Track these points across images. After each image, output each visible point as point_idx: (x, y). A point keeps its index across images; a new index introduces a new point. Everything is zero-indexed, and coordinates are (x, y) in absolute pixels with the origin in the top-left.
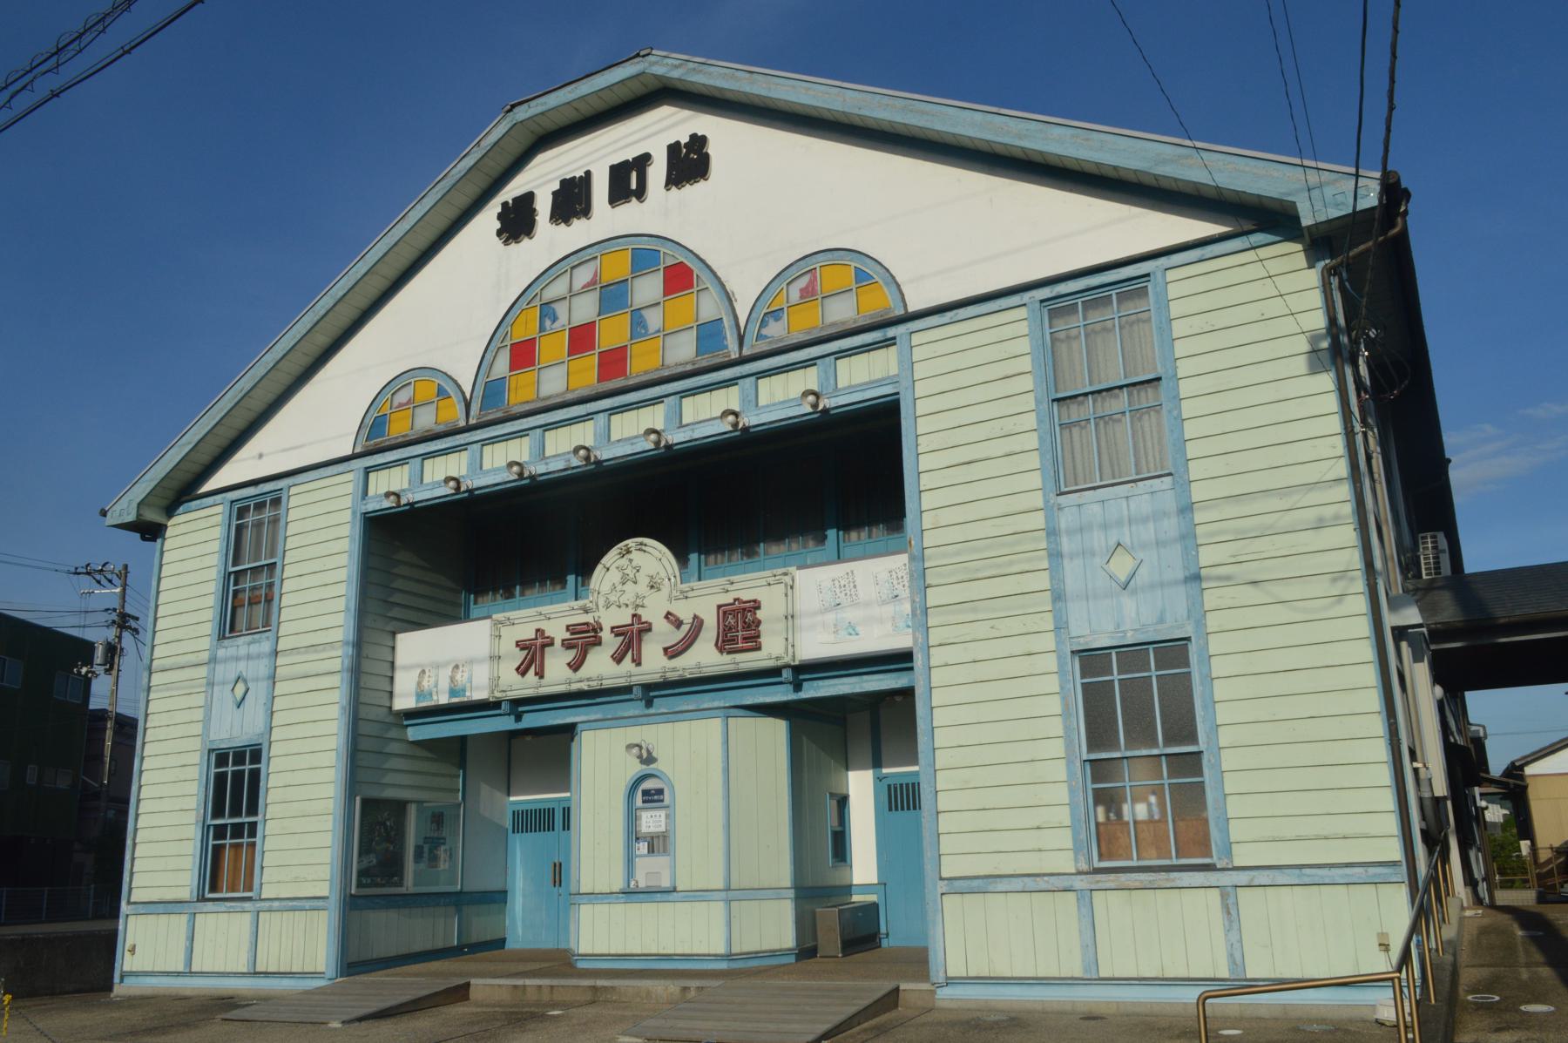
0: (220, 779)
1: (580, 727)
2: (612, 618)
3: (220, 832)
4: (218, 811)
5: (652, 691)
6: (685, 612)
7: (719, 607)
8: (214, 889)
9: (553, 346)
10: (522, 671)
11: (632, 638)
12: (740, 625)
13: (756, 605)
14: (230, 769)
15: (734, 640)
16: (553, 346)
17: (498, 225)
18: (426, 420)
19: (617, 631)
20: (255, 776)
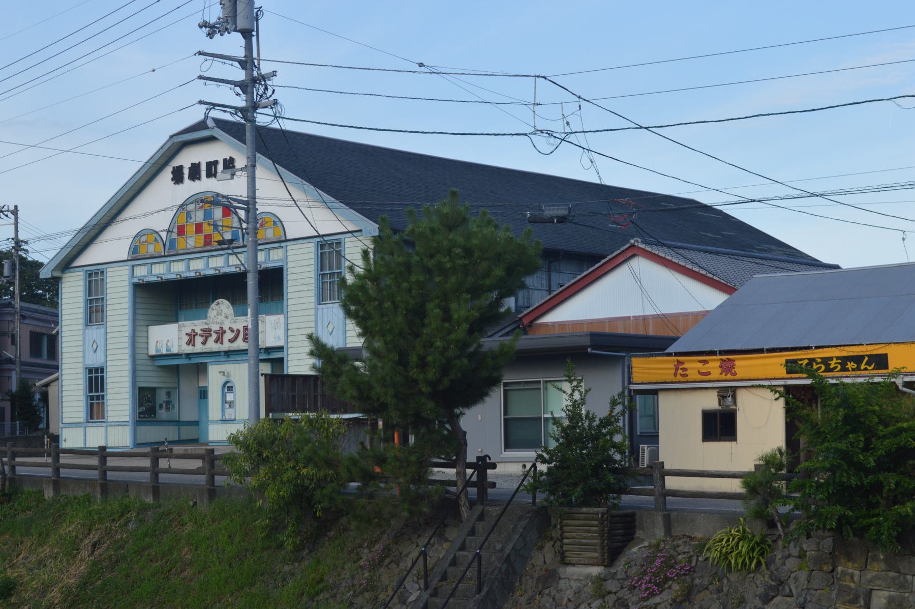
0: (90, 378)
2: (215, 327)
3: (92, 398)
4: (91, 391)
5: (228, 353)
8: (92, 418)
9: (190, 229)
10: (188, 343)
14: (94, 375)
16: (190, 229)
17: (171, 176)
18: (151, 249)
20: (102, 378)
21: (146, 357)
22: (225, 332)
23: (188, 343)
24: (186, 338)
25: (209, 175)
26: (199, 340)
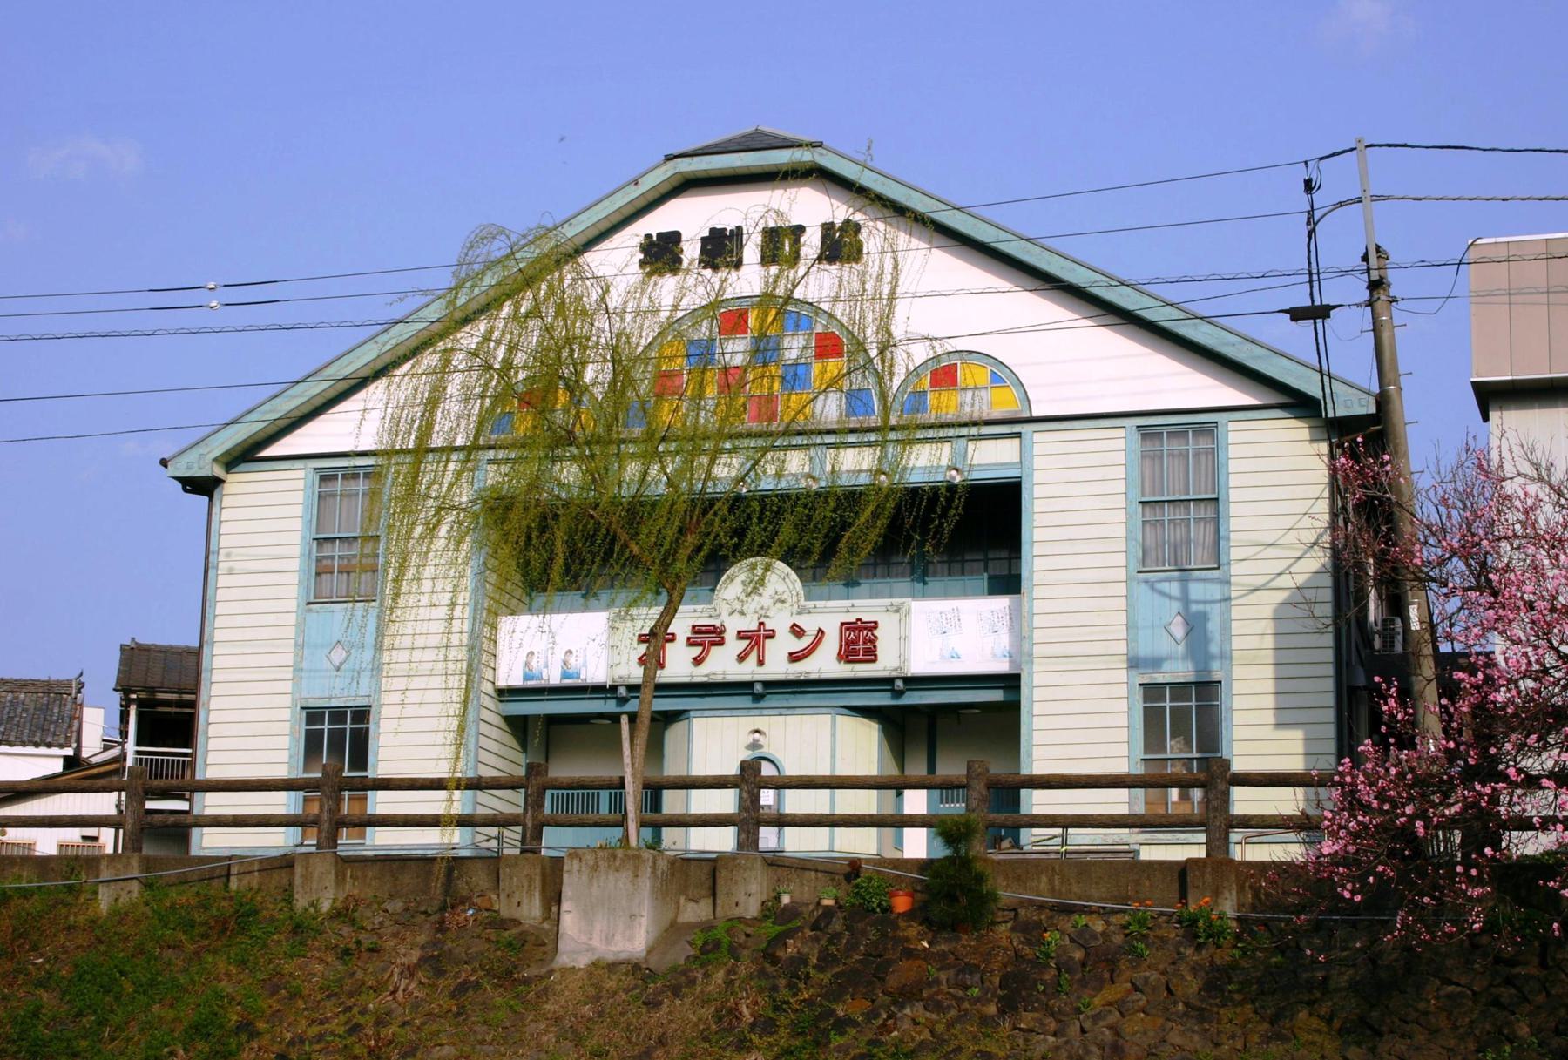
6: (810, 624)
11: (756, 639)
12: (859, 641)
19: (741, 635)
25: (771, 254)
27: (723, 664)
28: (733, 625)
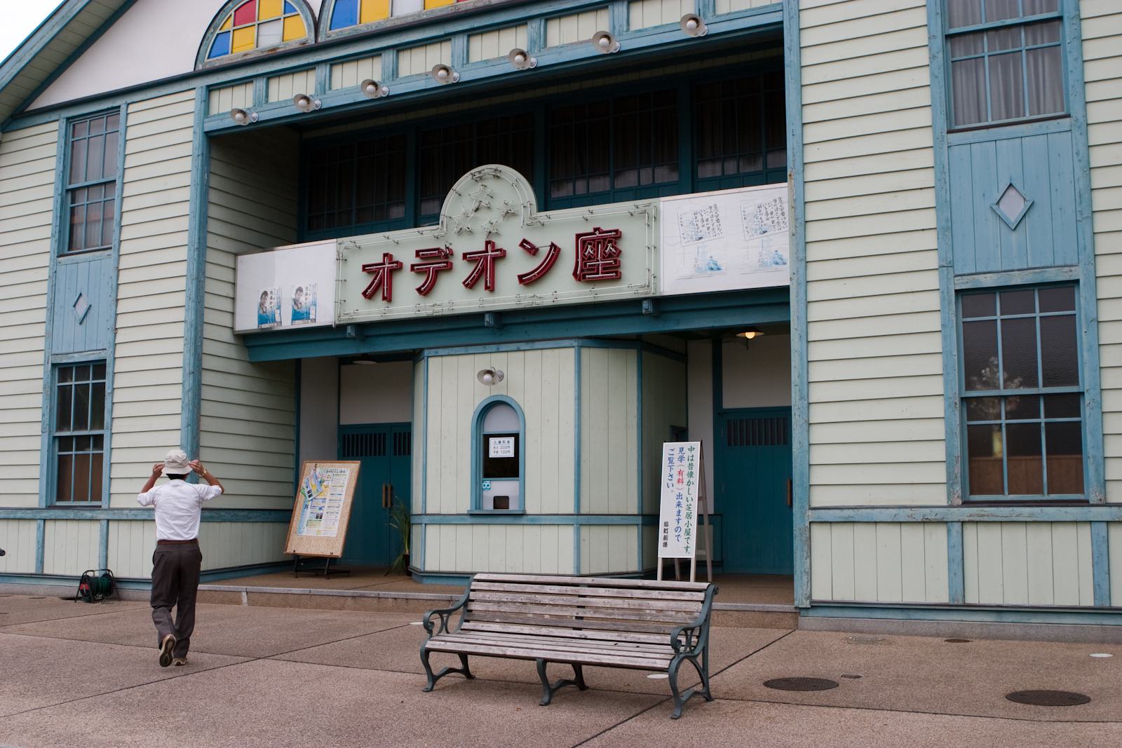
0: (64, 393)
1: (426, 353)
6: (542, 241)
7: (578, 236)
8: (60, 498)
10: (369, 295)
12: (600, 256)
13: (617, 235)
15: (594, 270)
20: (100, 391)
21: (227, 336)
22: (502, 255)
23: (369, 295)
24: (365, 281)
26: (406, 284)
27: (453, 296)
28: (461, 246)
